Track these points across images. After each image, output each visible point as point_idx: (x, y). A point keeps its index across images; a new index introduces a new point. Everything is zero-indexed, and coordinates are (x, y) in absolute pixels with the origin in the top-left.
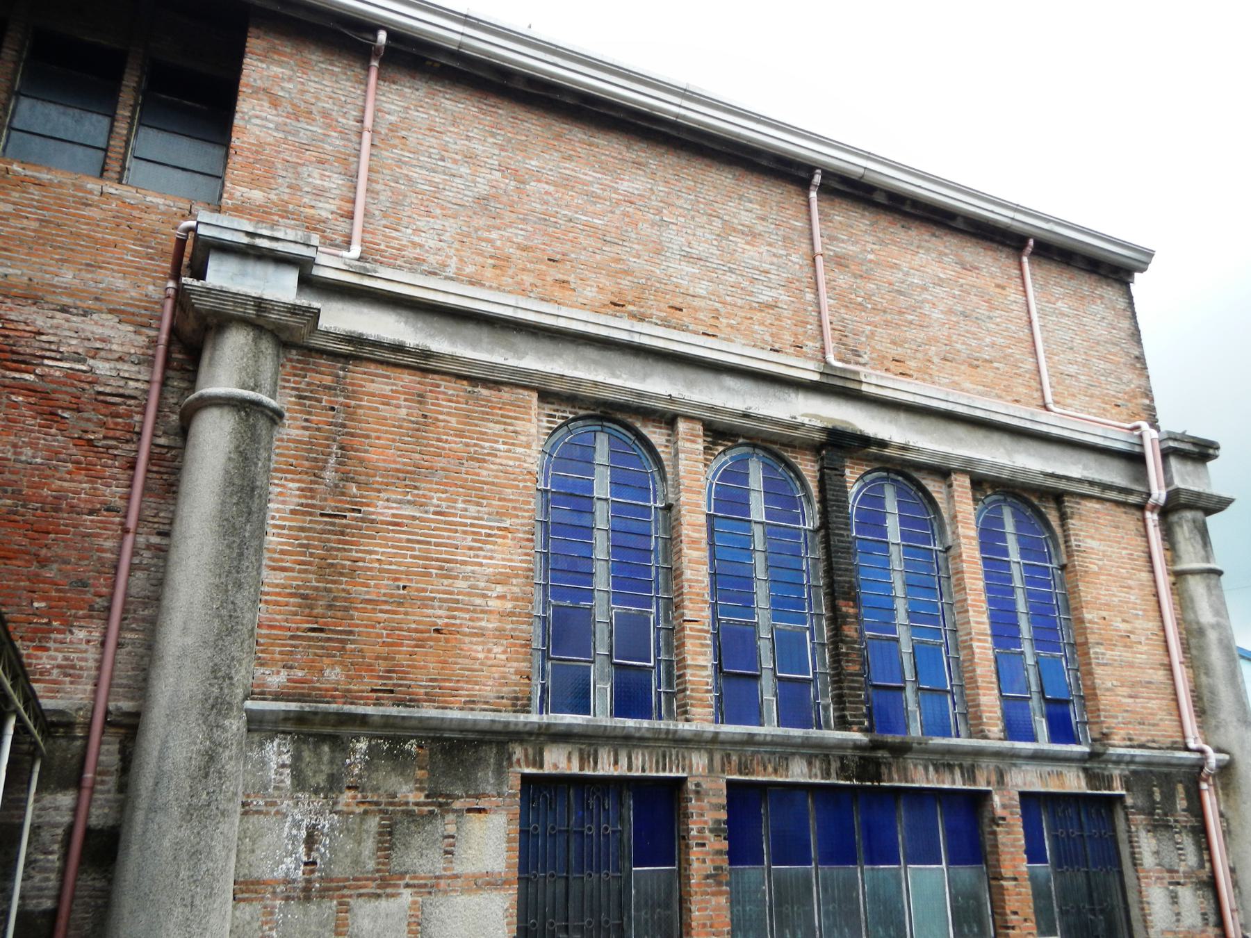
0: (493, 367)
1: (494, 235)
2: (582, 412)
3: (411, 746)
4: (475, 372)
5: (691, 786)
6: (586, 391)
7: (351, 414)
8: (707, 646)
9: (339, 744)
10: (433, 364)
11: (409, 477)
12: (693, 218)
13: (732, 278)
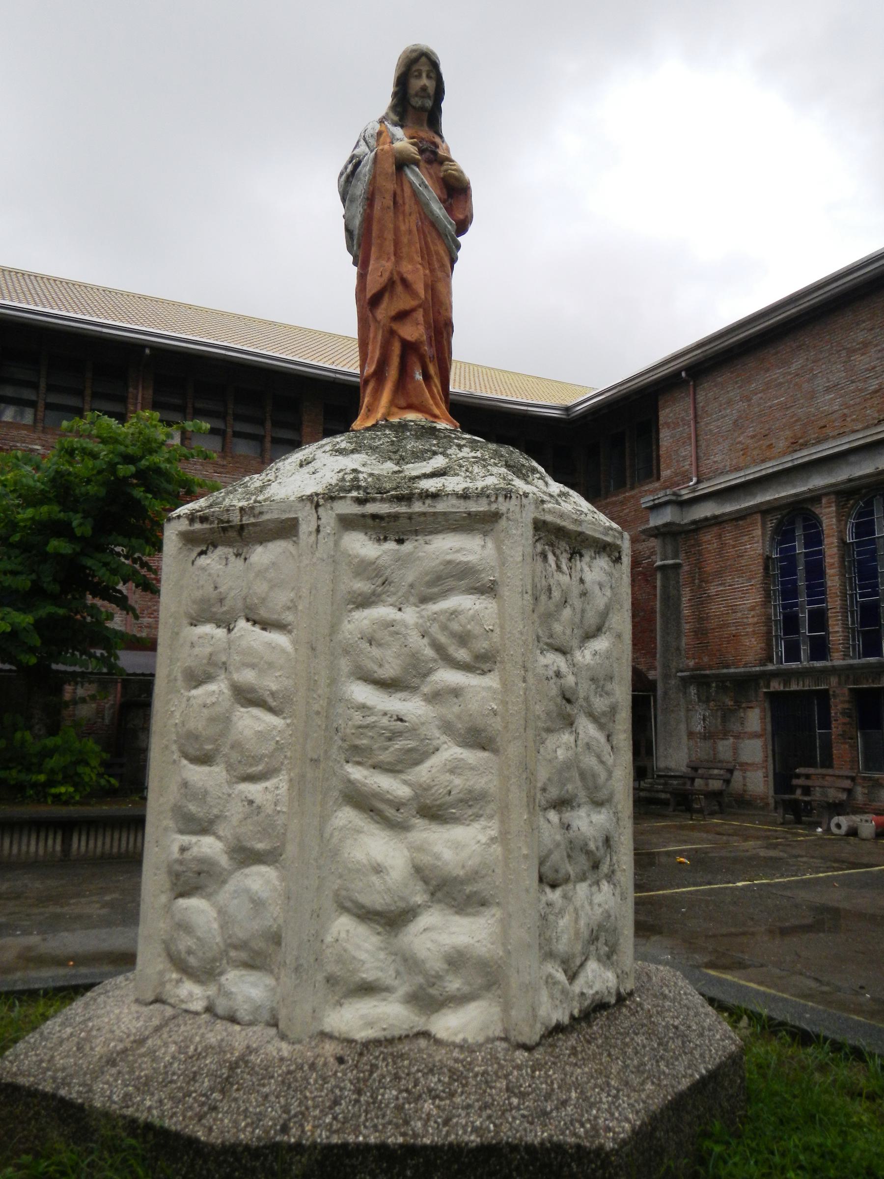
0: (737, 511)
1: (741, 439)
2: (785, 512)
3: (728, 684)
4: (734, 516)
5: (831, 693)
6: (777, 504)
7: (700, 553)
8: (839, 620)
9: (708, 685)
10: (720, 520)
11: (719, 573)
12: (829, 361)
13: (852, 387)
